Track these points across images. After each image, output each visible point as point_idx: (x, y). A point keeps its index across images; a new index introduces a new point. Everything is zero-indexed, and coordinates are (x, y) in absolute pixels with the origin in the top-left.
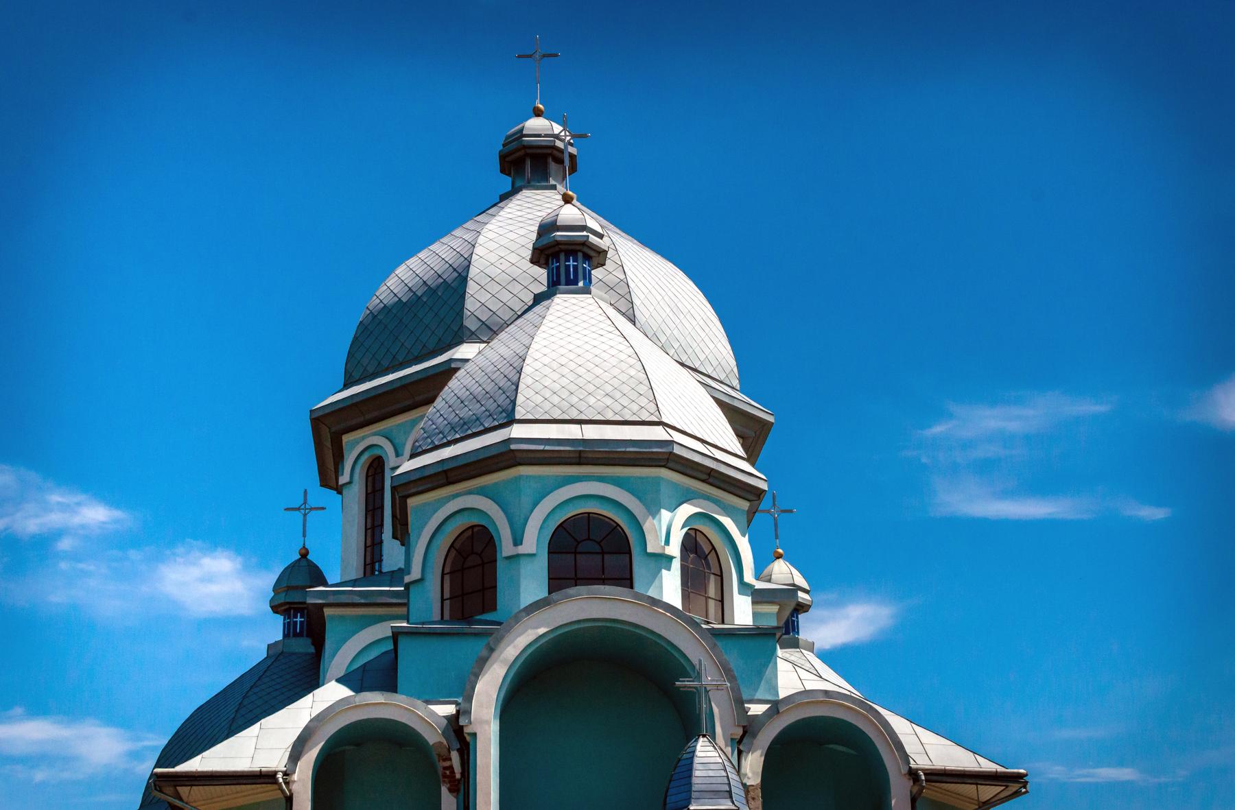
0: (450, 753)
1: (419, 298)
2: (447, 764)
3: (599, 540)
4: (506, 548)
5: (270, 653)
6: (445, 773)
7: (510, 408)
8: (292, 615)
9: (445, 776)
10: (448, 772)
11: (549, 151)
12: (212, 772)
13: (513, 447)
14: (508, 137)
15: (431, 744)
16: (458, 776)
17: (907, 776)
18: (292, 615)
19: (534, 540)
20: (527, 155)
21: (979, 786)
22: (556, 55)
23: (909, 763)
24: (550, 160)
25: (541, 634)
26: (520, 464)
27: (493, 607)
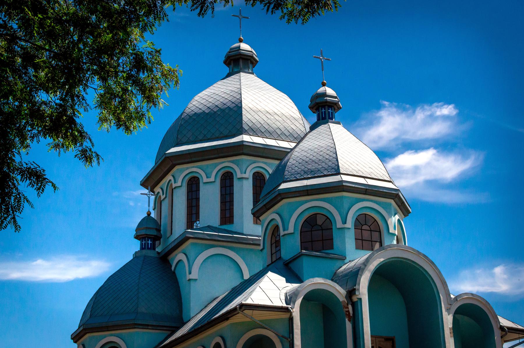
0: (348, 305)
1: (215, 112)
2: (347, 310)
3: (361, 226)
4: (339, 224)
5: (137, 255)
6: (347, 313)
7: (336, 167)
8: (147, 240)
9: (346, 315)
10: (347, 313)
11: (249, 58)
12: (264, 305)
13: (344, 184)
14: (231, 49)
15: (341, 301)
16: (351, 315)
17: (500, 329)
18: (147, 240)
19: (350, 223)
20: (241, 58)
21: (520, 335)
22: (248, 18)
23: (500, 324)
24: (249, 62)
25: (382, 261)
26: (344, 191)
27: (332, 248)
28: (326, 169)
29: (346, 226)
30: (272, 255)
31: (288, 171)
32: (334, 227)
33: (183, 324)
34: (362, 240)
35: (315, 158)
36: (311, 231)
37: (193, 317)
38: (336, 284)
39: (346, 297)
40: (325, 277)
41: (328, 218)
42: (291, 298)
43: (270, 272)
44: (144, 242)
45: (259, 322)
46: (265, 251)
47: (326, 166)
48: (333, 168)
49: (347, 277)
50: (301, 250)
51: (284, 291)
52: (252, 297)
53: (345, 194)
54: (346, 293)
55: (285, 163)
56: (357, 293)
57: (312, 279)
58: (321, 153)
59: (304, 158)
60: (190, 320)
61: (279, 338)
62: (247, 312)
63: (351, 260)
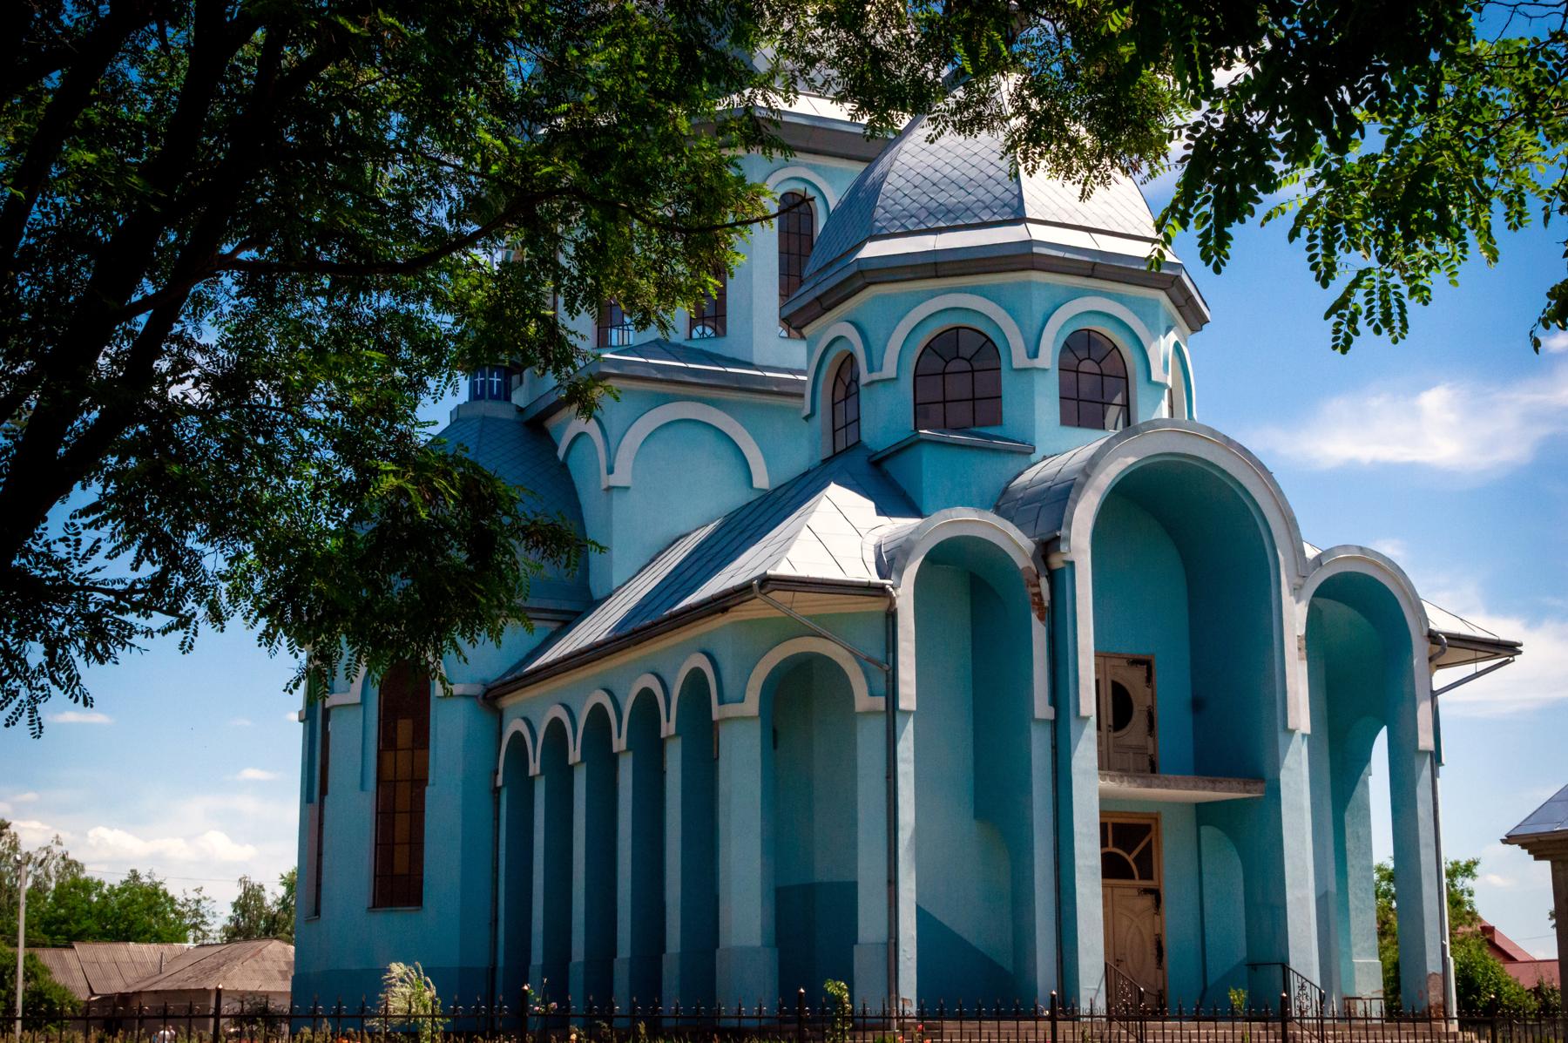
2: (1035, 590)
4: (1019, 359)
7: (1015, 202)
9: (1034, 603)
13: (1035, 250)
16: (1046, 604)
19: (1049, 356)
26: (1033, 269)
27: (997, 420)
28: (987, 207)
29: (1037, 363)
30: (834, 431)
31: (883, 208)
32: (1004, 367)
33: (588, 604)
34: (1078, 400)
35: (957, 173)
36: (944, 374)
37: (619, 588)
38: (1009, 524)
39: (1034, 558)
40: (982, 506)
41: (989, 339)
42: (892, 560)
43: (833, 485)
44: (479, 379)
45: (804, 620)
46: (818, 419)
47: (988, 198)
48: (1005, 205)
49: (1038, 505)
50: (916, 428)
51: (872, 540)
52: (790, 555)
53: (1036, 276)
54: (1033, 546)
55: (874, 184)
56: (1063, 548)
57: (945, 512)
58: (975, 160)
59: (928, 173)
60: (611, 596)
61: (861, 665)
62: (776, 595)
63: (1047, 454)
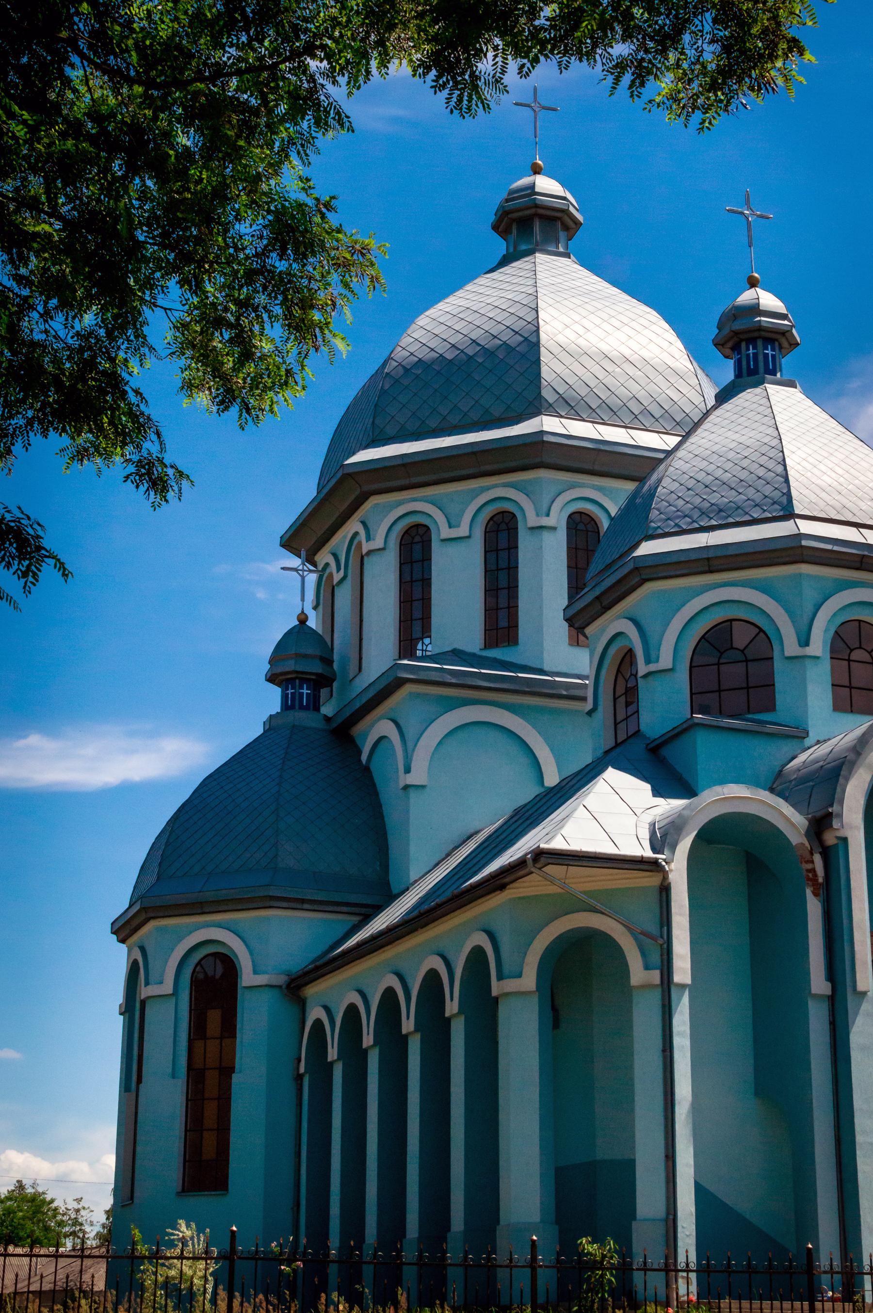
2: (809, 866)
4: (791, 647)
7: (784, 500)
9: (809, 879)
10: (810, 875)
13: (804, 543)
14: (512, 192)
16: (821, 880)
19: (819, 645)
22: (555, 110)
27: (770, 706)
28: (757, 505)
29: (810, 651)
30: (616, 724)
31: (658, 510)
32: (776, 654)
33: (390, 897)
34: (851, 687)
35: (728, 475)
36: (718, 664)
37: (416, 881)
38: (781, 801)
39: (807, 834)
40: (755, 782)
41: (761, 630)
42: (664, 836)
43: (610, 769)
44: (290, 691)
45: (583, 897)
46: (599, 715)
47: (758, 497)
48: (774, 503)
49: (811, 783)
50: (692, 713)
51: (647, 818)
52: (563, 832)
53: (806, 569)
54: (806, 823)
55: (650, 490)
56: (836, 824)
57: (718, 789)
58: (745, 463)
59: (701, 476)
60: (408, 889)
61: (636, 939)
62: (550, 869)
63: (821, 739)
